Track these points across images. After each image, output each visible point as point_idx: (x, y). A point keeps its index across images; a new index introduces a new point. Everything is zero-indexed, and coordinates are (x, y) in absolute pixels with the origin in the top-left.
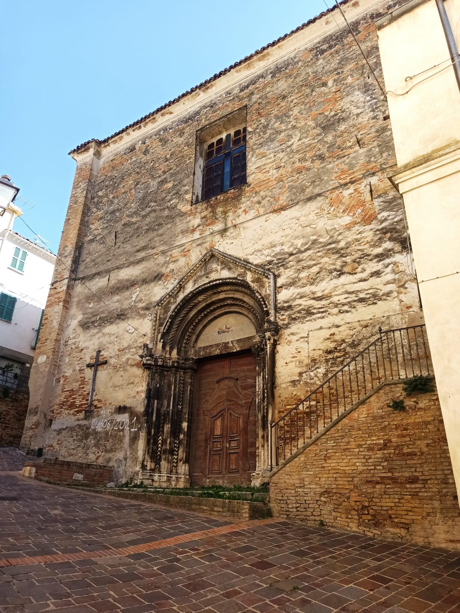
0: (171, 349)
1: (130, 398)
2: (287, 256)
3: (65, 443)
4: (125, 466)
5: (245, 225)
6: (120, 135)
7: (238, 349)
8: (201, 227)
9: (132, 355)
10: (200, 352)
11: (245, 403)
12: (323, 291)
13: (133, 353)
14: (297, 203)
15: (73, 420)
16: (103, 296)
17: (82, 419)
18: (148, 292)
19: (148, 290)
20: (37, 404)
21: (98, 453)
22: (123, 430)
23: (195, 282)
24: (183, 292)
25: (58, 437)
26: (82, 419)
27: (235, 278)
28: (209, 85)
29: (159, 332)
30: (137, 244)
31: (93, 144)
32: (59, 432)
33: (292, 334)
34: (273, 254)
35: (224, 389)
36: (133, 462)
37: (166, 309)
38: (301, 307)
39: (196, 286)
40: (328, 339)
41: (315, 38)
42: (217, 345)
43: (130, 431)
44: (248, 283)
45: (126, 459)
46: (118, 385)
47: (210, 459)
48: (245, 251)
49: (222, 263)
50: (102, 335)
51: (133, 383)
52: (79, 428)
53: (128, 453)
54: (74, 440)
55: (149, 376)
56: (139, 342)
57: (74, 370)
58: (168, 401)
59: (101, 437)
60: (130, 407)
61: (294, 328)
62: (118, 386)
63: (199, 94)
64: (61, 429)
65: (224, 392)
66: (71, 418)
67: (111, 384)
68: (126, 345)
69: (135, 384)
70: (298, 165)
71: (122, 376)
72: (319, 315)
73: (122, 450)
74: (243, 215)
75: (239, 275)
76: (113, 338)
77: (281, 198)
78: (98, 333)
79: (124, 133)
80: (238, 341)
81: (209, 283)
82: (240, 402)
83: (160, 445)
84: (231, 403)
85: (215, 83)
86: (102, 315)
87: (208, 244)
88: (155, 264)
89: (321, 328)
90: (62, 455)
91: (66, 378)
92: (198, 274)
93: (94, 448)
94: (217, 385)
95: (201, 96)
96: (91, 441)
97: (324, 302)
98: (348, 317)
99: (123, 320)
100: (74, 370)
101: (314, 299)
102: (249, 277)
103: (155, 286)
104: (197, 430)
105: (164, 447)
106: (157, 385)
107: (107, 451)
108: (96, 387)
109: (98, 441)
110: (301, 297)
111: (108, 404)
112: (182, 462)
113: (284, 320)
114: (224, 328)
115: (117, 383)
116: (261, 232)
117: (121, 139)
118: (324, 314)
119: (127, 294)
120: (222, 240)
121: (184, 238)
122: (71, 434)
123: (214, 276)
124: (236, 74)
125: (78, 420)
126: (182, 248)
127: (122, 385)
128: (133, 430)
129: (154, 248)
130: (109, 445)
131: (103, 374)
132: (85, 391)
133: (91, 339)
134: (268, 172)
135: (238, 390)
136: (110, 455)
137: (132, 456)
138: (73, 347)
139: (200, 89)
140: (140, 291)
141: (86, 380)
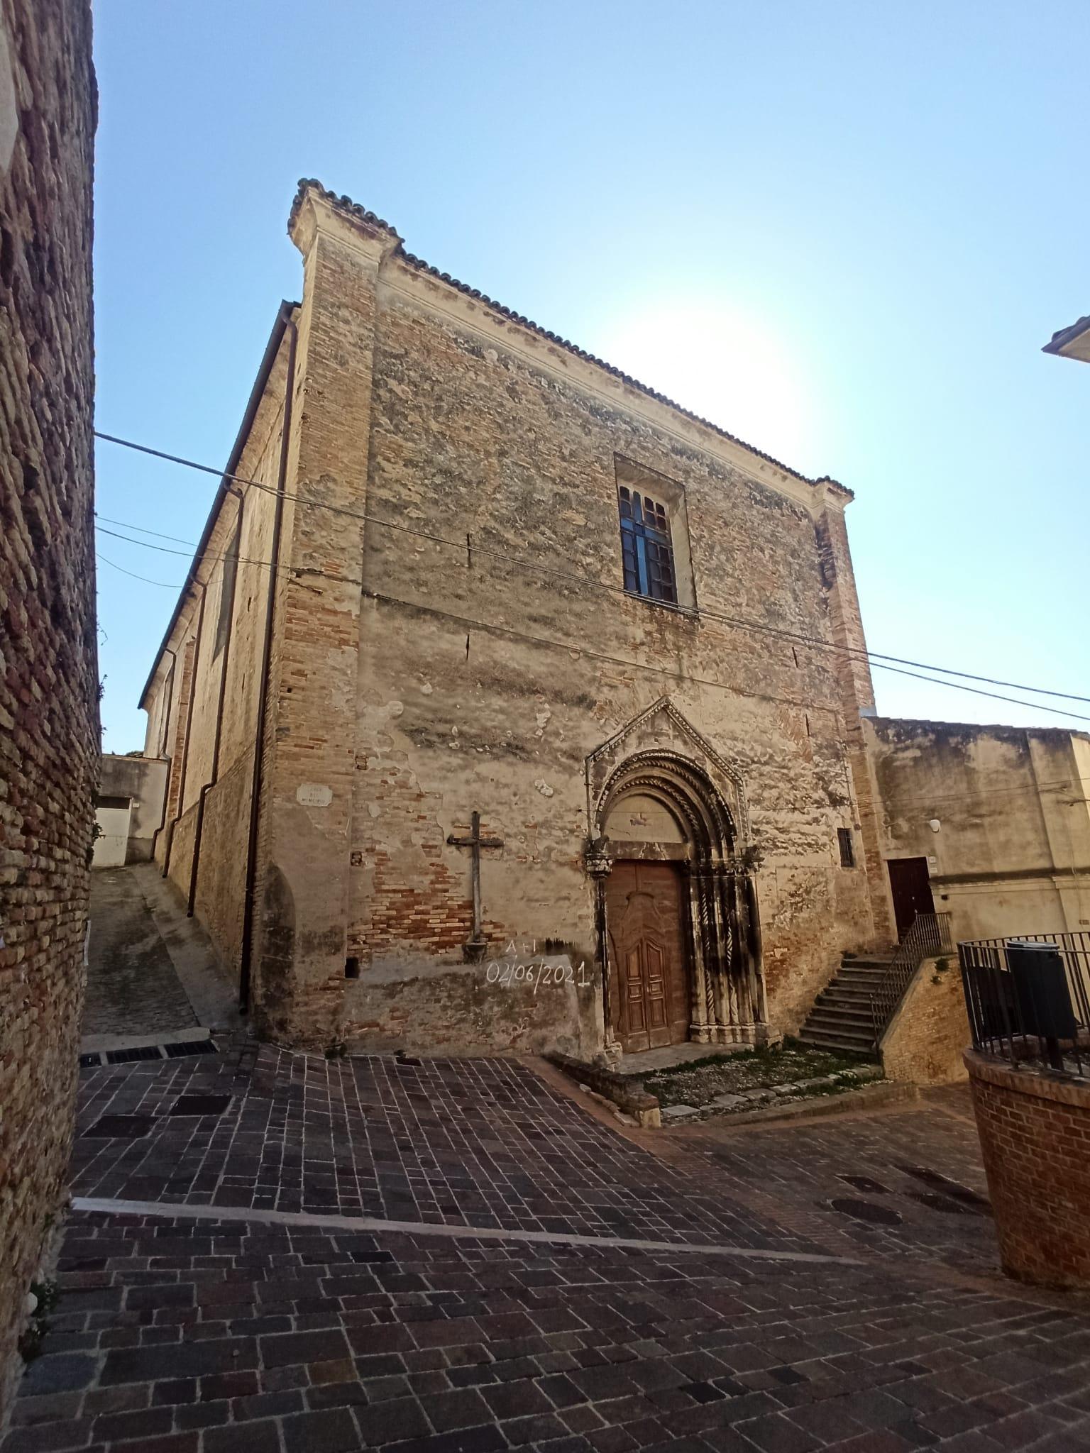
1: (566, 926)
3: (417, 1016)
4: (579, 1047)
5: (705, 687)
6: (454, 290)
9: (557, 843)
13: (558, 840)
14: (754, 695)
15: (433, 963)
16: (459, 682)
17: (458, 963)
18: (571, 724)
19: (570, 719)
20: (332, 924)
21: (515, 1029)
22: (562, 985)
23: (640, 739)
25: (390, 1002)
27: (693, 761)
28: (636, 390)
30: (527, 600)
31: (392, 244)
32: (392, 990)
36: (591, 1039)
41: (750, 472)
42: (640, 844)
43: (578, 988)
45: (577, 1036)
46: (536, 897)
49: (675, 727)
50: (473, 776)
51: (567, 898)
52: (452, 981)
53: (581, 1025)
54: (445, 1008)
56: (566, 819)
57: (407, 842)
59: (515, 1000)
60: (570, 944)
62: (537, 901)
63: (617, 387)
64: (395, 984)
65: (640, 914)
66: (423, 959)
67: (519, 894)
68: (540, 818)
69: (572, 900)
71: (542, 881)
72: (782, 850)
73: (567, 1022)
74: (700, 670)
76: (505, 792)
78: (463, 768)
85: (645, 399)
86: (465, 728)
88: (575, 670)
89: (785, 866)
90: (414, 1044)
91: (383, 859)
93: (503, 1022)
96: (492, 1008)
98: (801, 861)
99: (525, 761)
100: (407, 842)
101: (777, 829)
102: (709, 768)
103: (582, 715)
107: (534, 1025)
109: (511, 1007)
110: (768, 823)
111: (519, 934)
116: (720, 709)
117: (449, 296)
119: (523, 704)
120: (677, 691)
123: (665, 743)
124: (669, 416)
125: (446, 963)
126: (621, 667)
127: (546, 899)
128: (581, 985)
129: (567, 634)
130: (537, 1014)
132: (451, 899)
133: (445, 778)
136: (544, 1032)
137: (588, 1029)
138: (391, 781)
139: (624, 381)
140: (552, 713)
141: (449, 874)
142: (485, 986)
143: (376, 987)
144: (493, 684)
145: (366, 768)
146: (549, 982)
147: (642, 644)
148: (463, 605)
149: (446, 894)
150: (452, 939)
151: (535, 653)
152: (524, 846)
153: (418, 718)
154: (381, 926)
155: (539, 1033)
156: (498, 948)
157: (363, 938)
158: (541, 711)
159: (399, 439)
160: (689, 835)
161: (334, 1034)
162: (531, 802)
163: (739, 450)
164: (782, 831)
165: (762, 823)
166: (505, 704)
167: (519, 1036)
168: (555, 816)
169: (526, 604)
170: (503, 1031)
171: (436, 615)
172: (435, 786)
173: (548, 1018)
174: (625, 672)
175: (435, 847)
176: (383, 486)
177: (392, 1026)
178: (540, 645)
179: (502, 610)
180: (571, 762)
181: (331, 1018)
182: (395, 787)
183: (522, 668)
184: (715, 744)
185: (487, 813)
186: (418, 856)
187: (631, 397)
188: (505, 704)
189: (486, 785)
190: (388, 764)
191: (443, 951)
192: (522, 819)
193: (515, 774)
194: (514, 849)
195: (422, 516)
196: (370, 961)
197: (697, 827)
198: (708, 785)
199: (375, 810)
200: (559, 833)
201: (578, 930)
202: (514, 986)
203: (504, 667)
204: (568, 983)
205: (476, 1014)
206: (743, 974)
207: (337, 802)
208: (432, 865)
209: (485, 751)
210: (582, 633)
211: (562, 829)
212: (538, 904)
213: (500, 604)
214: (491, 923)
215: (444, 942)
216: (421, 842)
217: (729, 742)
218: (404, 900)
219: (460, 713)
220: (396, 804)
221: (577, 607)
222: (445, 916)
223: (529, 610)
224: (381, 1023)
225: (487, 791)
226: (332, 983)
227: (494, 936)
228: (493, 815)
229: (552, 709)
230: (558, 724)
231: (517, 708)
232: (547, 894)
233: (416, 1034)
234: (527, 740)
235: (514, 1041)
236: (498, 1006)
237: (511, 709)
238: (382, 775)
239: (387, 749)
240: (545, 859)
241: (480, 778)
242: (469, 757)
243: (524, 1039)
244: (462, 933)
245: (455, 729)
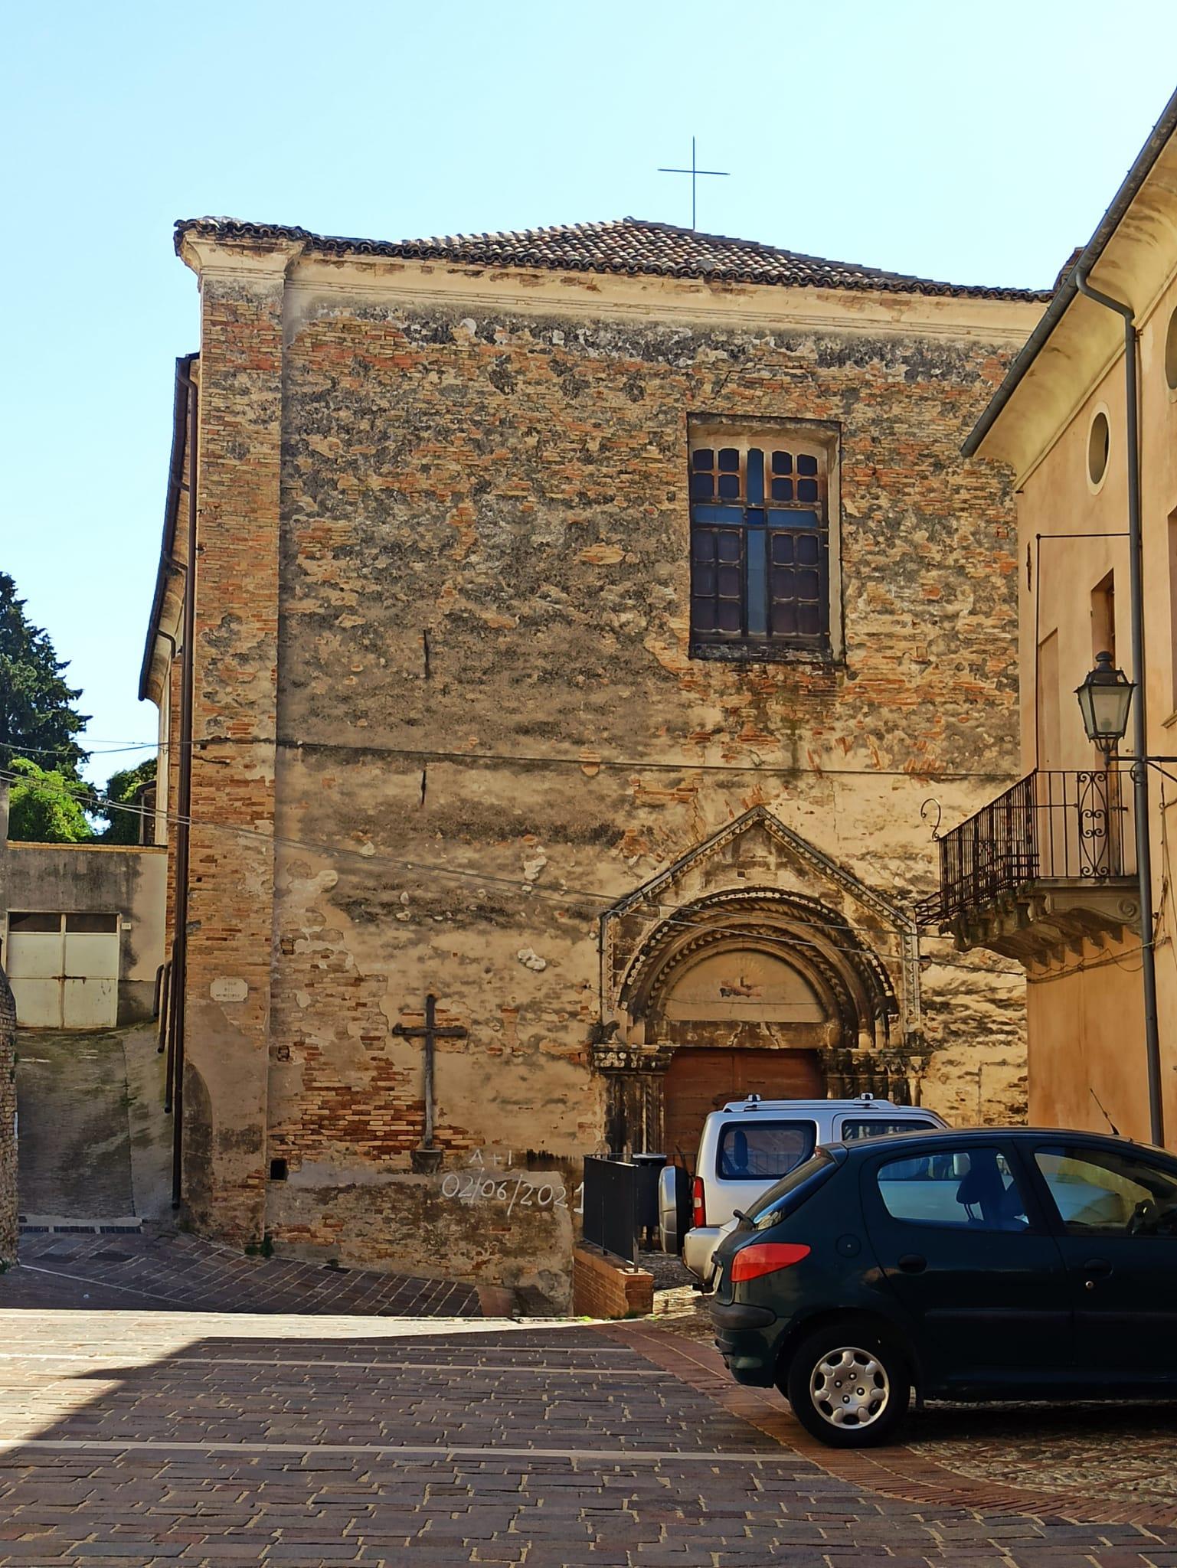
5: (846, 778)
7: (784, 1045)
8: (725, 737)
9: (549, 1030)
12: (1010, 990)
13: (550, 1026)
14: (964, 777)
15: (374, 1169)
16: (412, 835)
17: (405, 1171)
18: (579, 870)
19: (578, 863)
21: (479, 1254)
22: (549, 1208)
23: (708, 877)
26: (405, 1171)
27: (816, 901)
30: (514, 704)
32: (325, 1195)
33: (951, 1062)
34: (908, 876)
37: (630, 929)
38: (968, 1013)
39: (713, 889)
40: (1015, 1086)
42: (731, 1025)
44: (845, 921)
48: (842, 843)
49: (781, 850)
50: (430, 952)
51: (563, 1101)
52: (396, 1192)
54: (388, 1220)
55: (608, 1090)
56: (565, 999)
57: (343, 1034)
59: (481, 1220)
60: (564, 1159)
61: (955, 1050)
62: (515, 1103)
64: (328, 1189)
67: (491, 1094)
68: (523, 999)
70: (966, 676)
71: (524, 1079)
72: (1002, 1037)
74: (839, 751)
75: (823, 895)
76: (472, 970)
77: (930, 746)
78: (414, 943)
79: (416, 263)
80: (784, 1026)
81: (748, 890)
85: (755, 292)
86: (419, 893)
87: (749, 792)
88: (590, 792)
89: (1004, 1063)
90: (350, 1254)
91: (313, 1052)
92: (716, 859)
93: (462, 1244)
95: (700, 295)
96: (448, 1226)
97: (1010, 1014)
99: (504, 927)
101: (993, 1001)
102: (849, 909)
107: (506, 1252)
108: (438, 1094)
109: (475, 1228)
110: (968, 992)
111: (489, 1142)
113: (934, 1030)
114: (737, 984)
115: (508, 1093)
116: (880, 811)
117: (392, 268)
118: (1010, 1038)
119: (503, 852)
120: (785, 795)
121: (677, 749)
122: (373, 1204)
123: (757, 877)
124: (813, 301)
125: (390, 1170)
126: (673, 775)
127: (528, 1101)
129: (579, 742)
130: (511, 1238)
131: (450, 1060)
132: (397, 1098)
133: (391, 956)
134: (899, 660)
136: (521, 1261)
138: (323, 965)
139: (707, 281)
140: (549, 858)
141: (395, 1069)
142: (440, 1200)
143: (307, 1190)
144: (459, 831)
145: (293, 952)
146: (530, 1203)
147: (718, 730)
148: (417, 732)
149: (391, 1093)
150: (397, 1144)
151: (524, 778)
152: (499, 1035)
153: (356, 887)
154: (312, 1127)
155: (512, 1262)
156: (458, 1157)
157: (292, 1138)
158: (529, 858)
159: (327, 522)
160: (831, 1011)
161: (253, 1231)
162: (512, 979)
163: (984, 307)
164: (1003, 1004)
165: (956, 993)
166: (476, 856)
167: (485, 1262)
168: (547, 996)
169: (514, 711)
170: (463, 1254)
171: (380, 754)
172: (378, 967)
173: (527, 1245)
174: (681, 780)
175: (378, 1038)
176: (307, 596)
177: (326, 1234)
178: (531, 767)
179: (475, 727)
180: (576, 922)
181: (250, 1215)
182: (328, 972)
183: (504, 804)
184: (860, 869)
185: (446, 996)
186: (355, 1049)
187: (729, 296)
188: (476, 856)
189: (447, 962)
190: (320, 946)
191: (387, 1157)
192: (498, 1001)
193: (488, 944)
194: (485, 1040)
195: (360, 621)
196: (300, 1163)
198: (849, 935)
199: (304, 998)
200: (555, 1018)
201: (576, 1142)
202: (478, 1202)
203: (476, 806)
204: (558, 1208)
205: (427, 1231)
207: (254, 995)
208: (374, 1059)
209: (446, 919)
210: (605, 734)
211: (557, 1012)
212: (516, 1107)
213: (473, 719)
214: (450, 1127)
215: (388, 1146)
216: (361, 1032)
217: (894, 865)
218: (340, 1098)
219: (411, 876)
220: (329, 992)
221: (598, 698)
222: (389, 1118)
223: (517, 718)
224: (313, 1229)
225: (448, 970)
226: (251, 1182)
227: (453, 1143)
228: (456, 997)
229: (549, 852)
230: (557, 873)
231: (493, 859)
232: (530, 1095)
233: (353, 1244)
234: (507, 899)
235: (478, 1266)
236: (457, 1225)
237: (487, 860)
239: (317, 929)
240: (529, 1051)
241: (440, 954)
242: (423, 929)
243: (491, 1267)
244: (411, 1138)
245: (405, 895)
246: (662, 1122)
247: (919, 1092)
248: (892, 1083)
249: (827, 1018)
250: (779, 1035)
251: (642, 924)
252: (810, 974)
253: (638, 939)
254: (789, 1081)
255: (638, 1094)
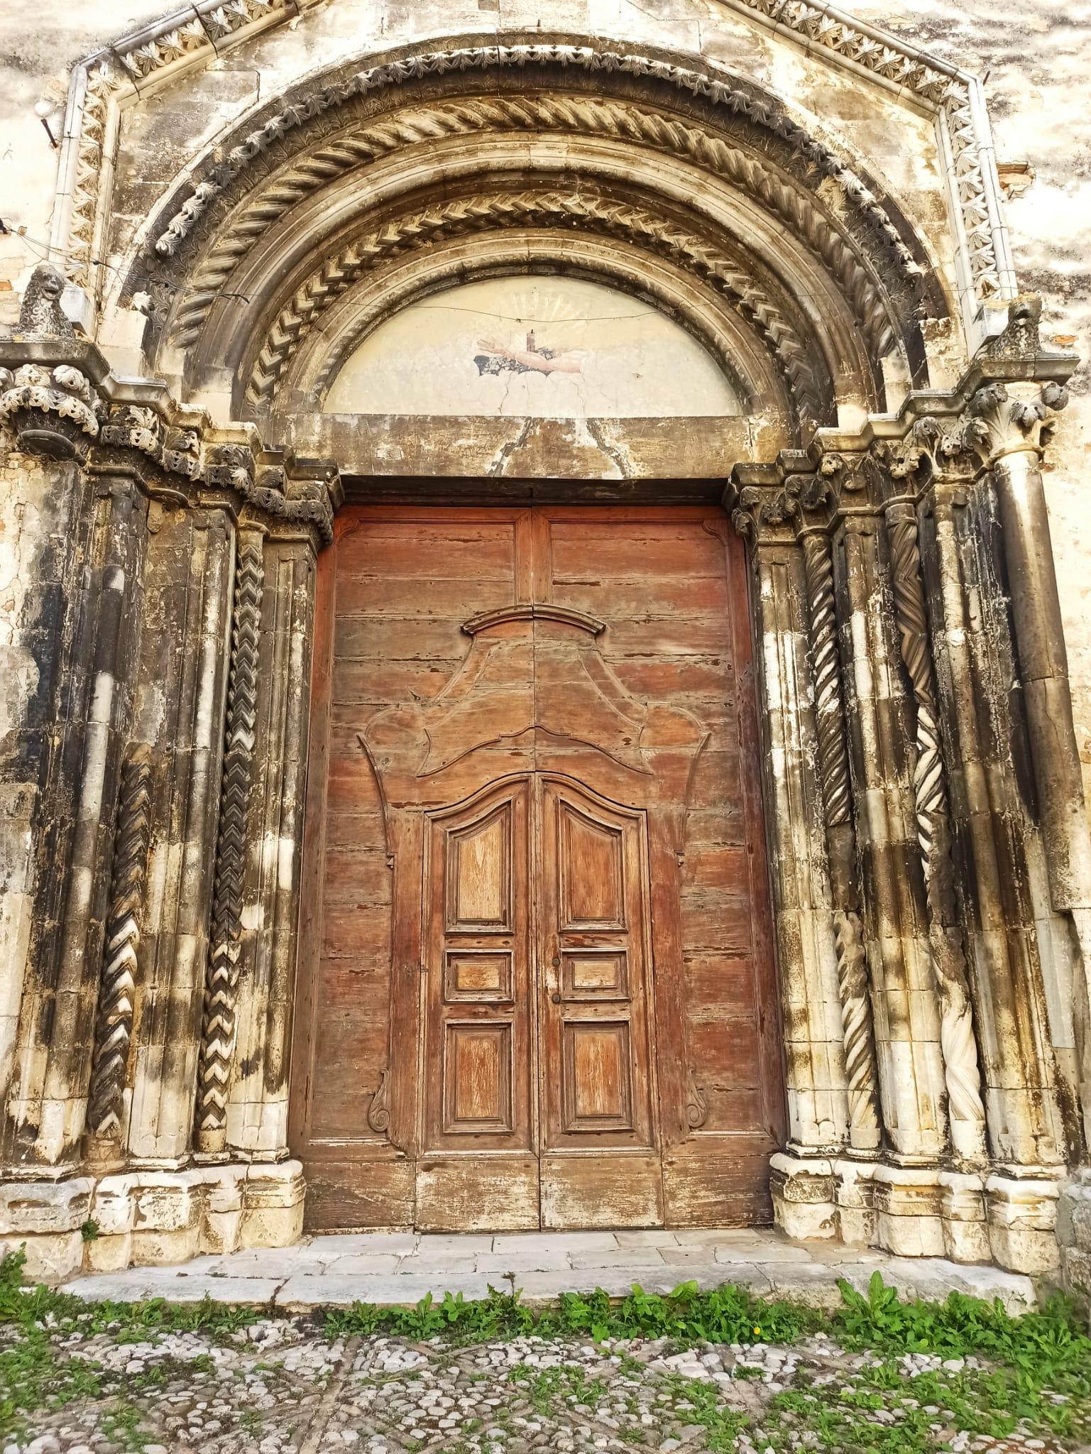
0: (197, 375)
2: (1033, 21)
7: (637, 471)
10: (374, 440)
11: (660, 762)
24: (309, 44)
27: (695, 62)
29: (115, 245)
35: (516, 673)
39: (408, 34)
42: (496, 426)
44: (777, 104)
47: (431, 1054)
55: (49, 504)
58: (175, 694)
65: (522, 691)
80: (637, 427)
82: (629, 755)
83: (126, 980)
84: (569, 751)
94: (462, 647)
104: (330, 879)
105: (153, 991)
106: (108, 575)
112: (257, 1079)
114: (518, 347)
135: (608, 689)
160: (759, 389)
197: (787, 347)
206: (991, 913)
238: (161, 528)
246: (297, 659)
247: (1042, 512)
248: (945, 497)
249: (749, 409)
250: (623, 448)
251: (208, 109)
252: (704, 310)
253: (192, 144)
254: (663, 579)
255: (198, 558)
